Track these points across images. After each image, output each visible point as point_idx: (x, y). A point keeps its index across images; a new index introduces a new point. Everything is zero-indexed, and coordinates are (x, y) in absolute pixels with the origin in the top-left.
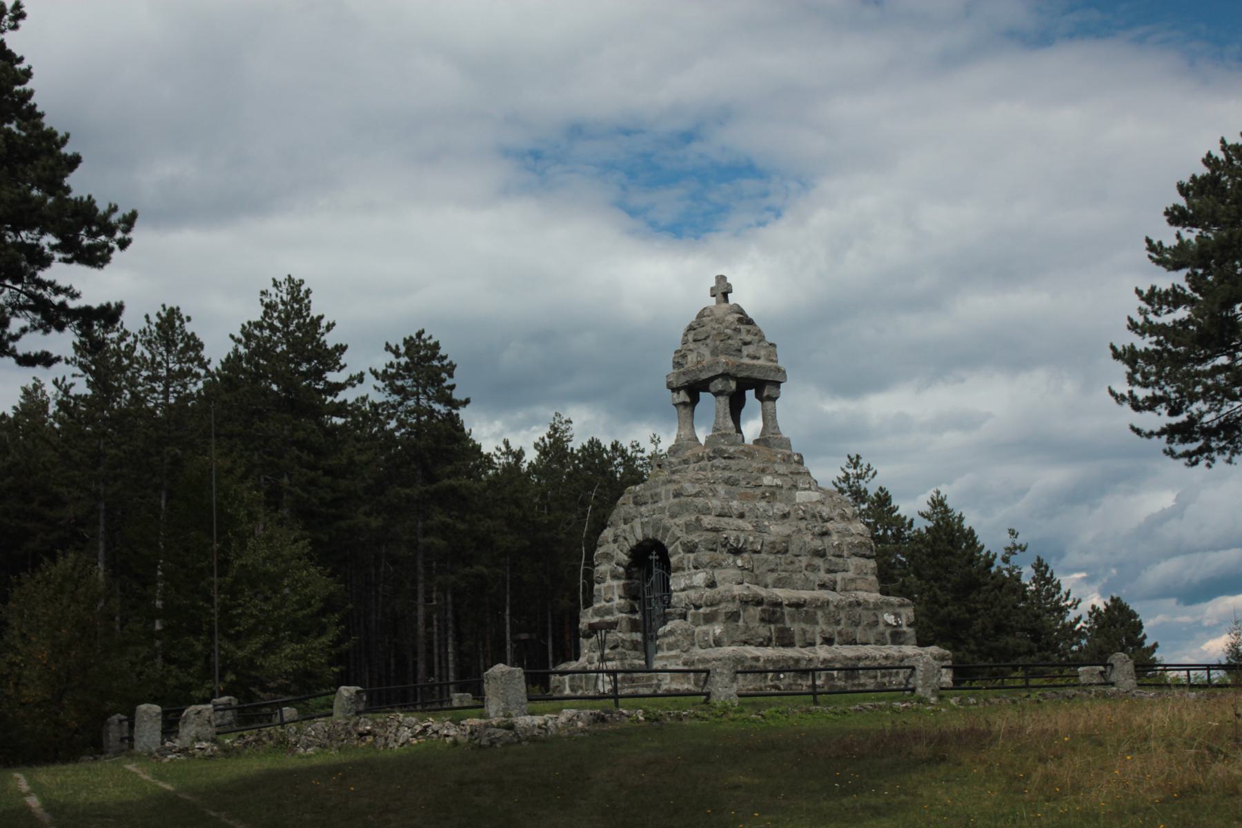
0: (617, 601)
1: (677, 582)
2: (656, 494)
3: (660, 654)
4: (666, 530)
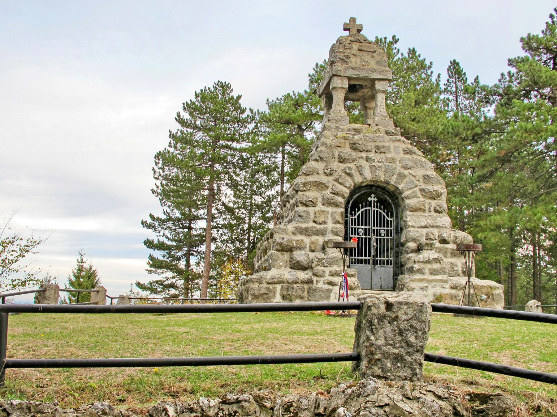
0: (330, 225)
1: (411, 218)
2: (383, 147)
3: (418, 276)
4: (401, 176)
